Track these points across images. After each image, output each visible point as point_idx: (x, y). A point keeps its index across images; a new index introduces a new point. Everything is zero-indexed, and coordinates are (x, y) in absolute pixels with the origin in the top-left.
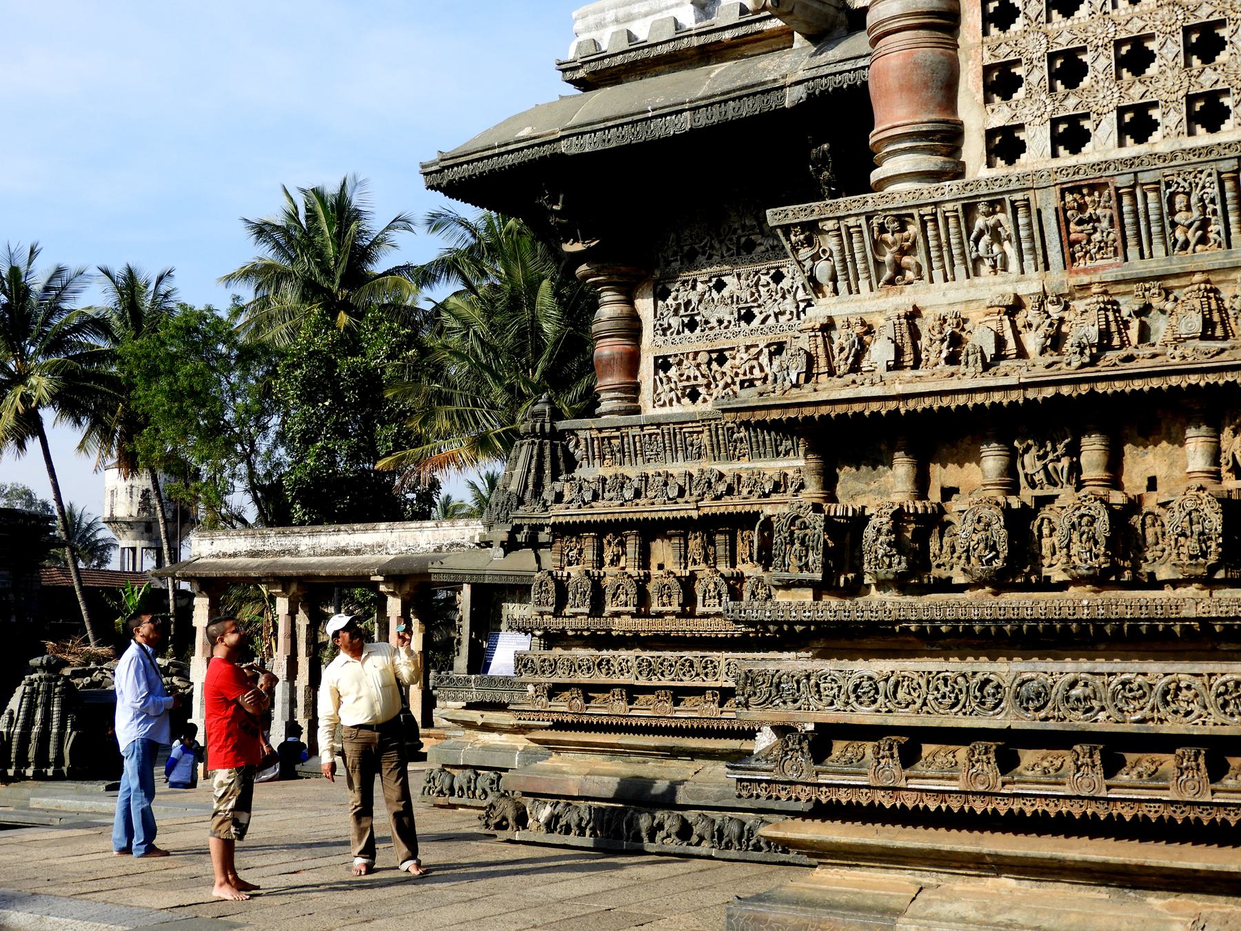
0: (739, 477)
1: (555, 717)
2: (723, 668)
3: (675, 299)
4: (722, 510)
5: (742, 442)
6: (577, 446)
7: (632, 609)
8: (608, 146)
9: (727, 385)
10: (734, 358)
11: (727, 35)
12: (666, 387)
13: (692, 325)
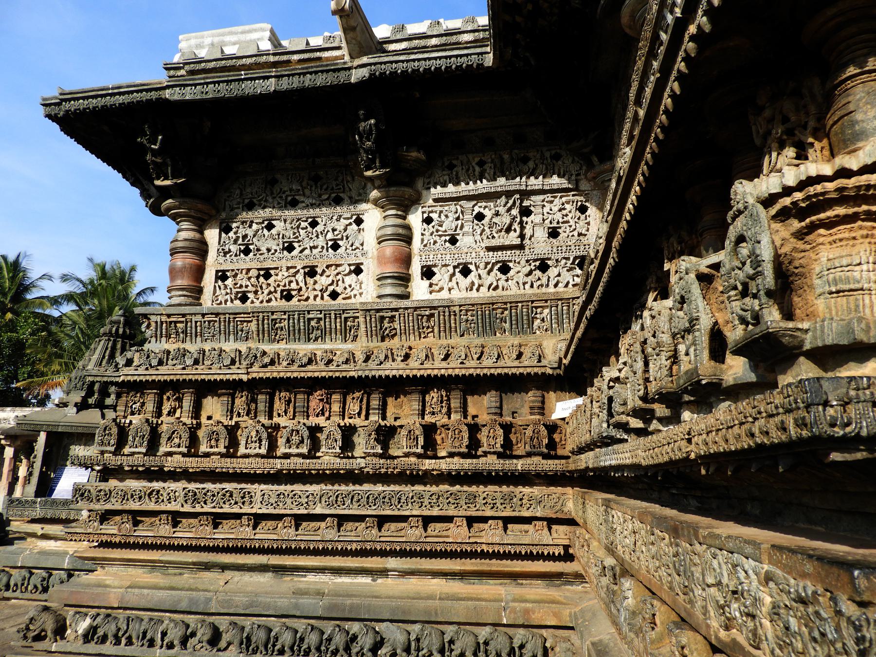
0: (279, 355)
1: (104, 538)
2: (258, 498)
3: (236, 233)
4: (268, 375)
5: (282, 329)
6: (148, 327)
7: (184, 450)
8: (204, 96)
9: (270, 293)
10: (277, 275)
11: (296, 57)
12: (223, 292)
13: (247, 251)
